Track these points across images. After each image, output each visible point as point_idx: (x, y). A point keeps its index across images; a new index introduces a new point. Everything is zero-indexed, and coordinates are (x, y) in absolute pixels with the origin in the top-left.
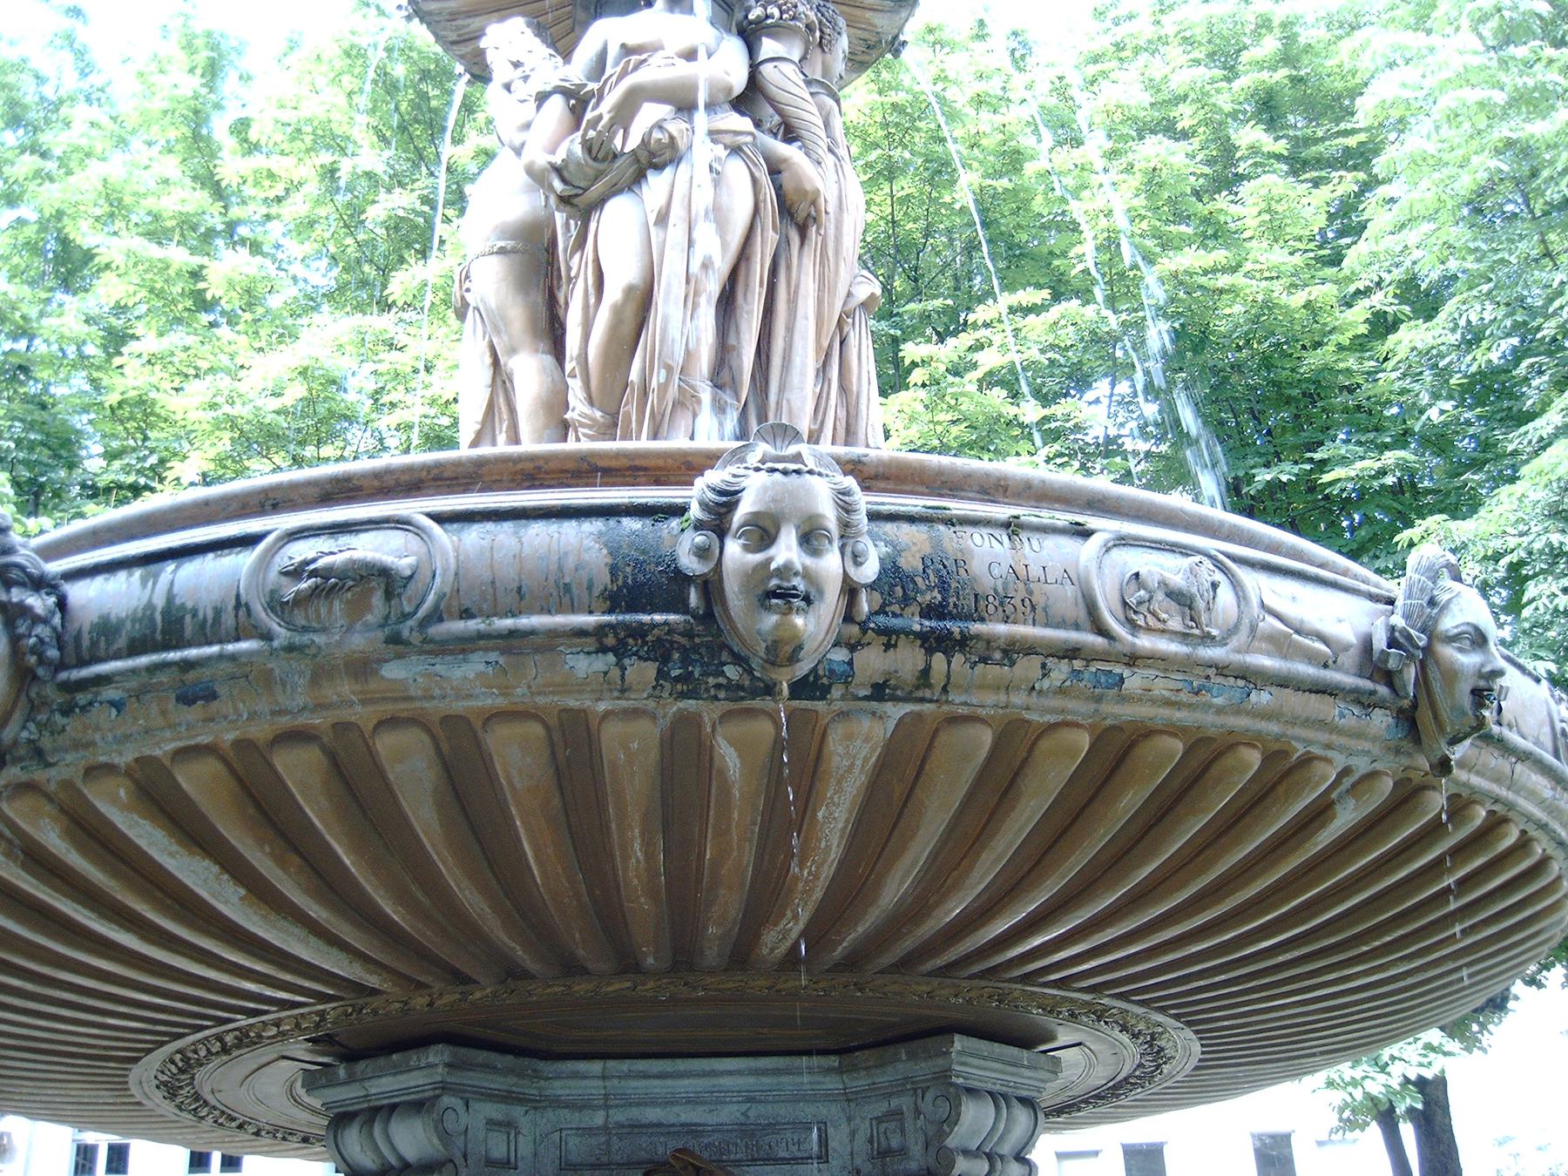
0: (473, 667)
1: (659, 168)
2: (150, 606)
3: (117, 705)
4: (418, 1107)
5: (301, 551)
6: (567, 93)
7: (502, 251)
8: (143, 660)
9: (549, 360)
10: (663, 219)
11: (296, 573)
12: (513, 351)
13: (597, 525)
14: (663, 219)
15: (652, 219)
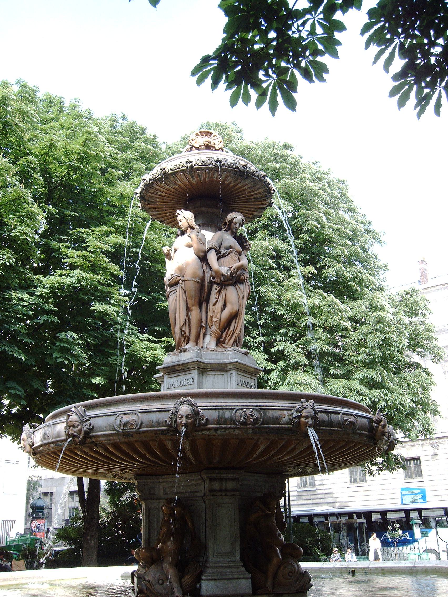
0: (357, 437)
1: (240, 283)
2: (329, 420)
3: (322, 433)
4: (233, 480)
5: (346, 417)
6: (216, 251)
7: (198, 282)
8: (328, 428)
9: (199, 310)
10: (243, 298)
11: (346, 421)
12: (193, 305)
13: (366, 420)
14: (243, 298)
15: (241, 296)
